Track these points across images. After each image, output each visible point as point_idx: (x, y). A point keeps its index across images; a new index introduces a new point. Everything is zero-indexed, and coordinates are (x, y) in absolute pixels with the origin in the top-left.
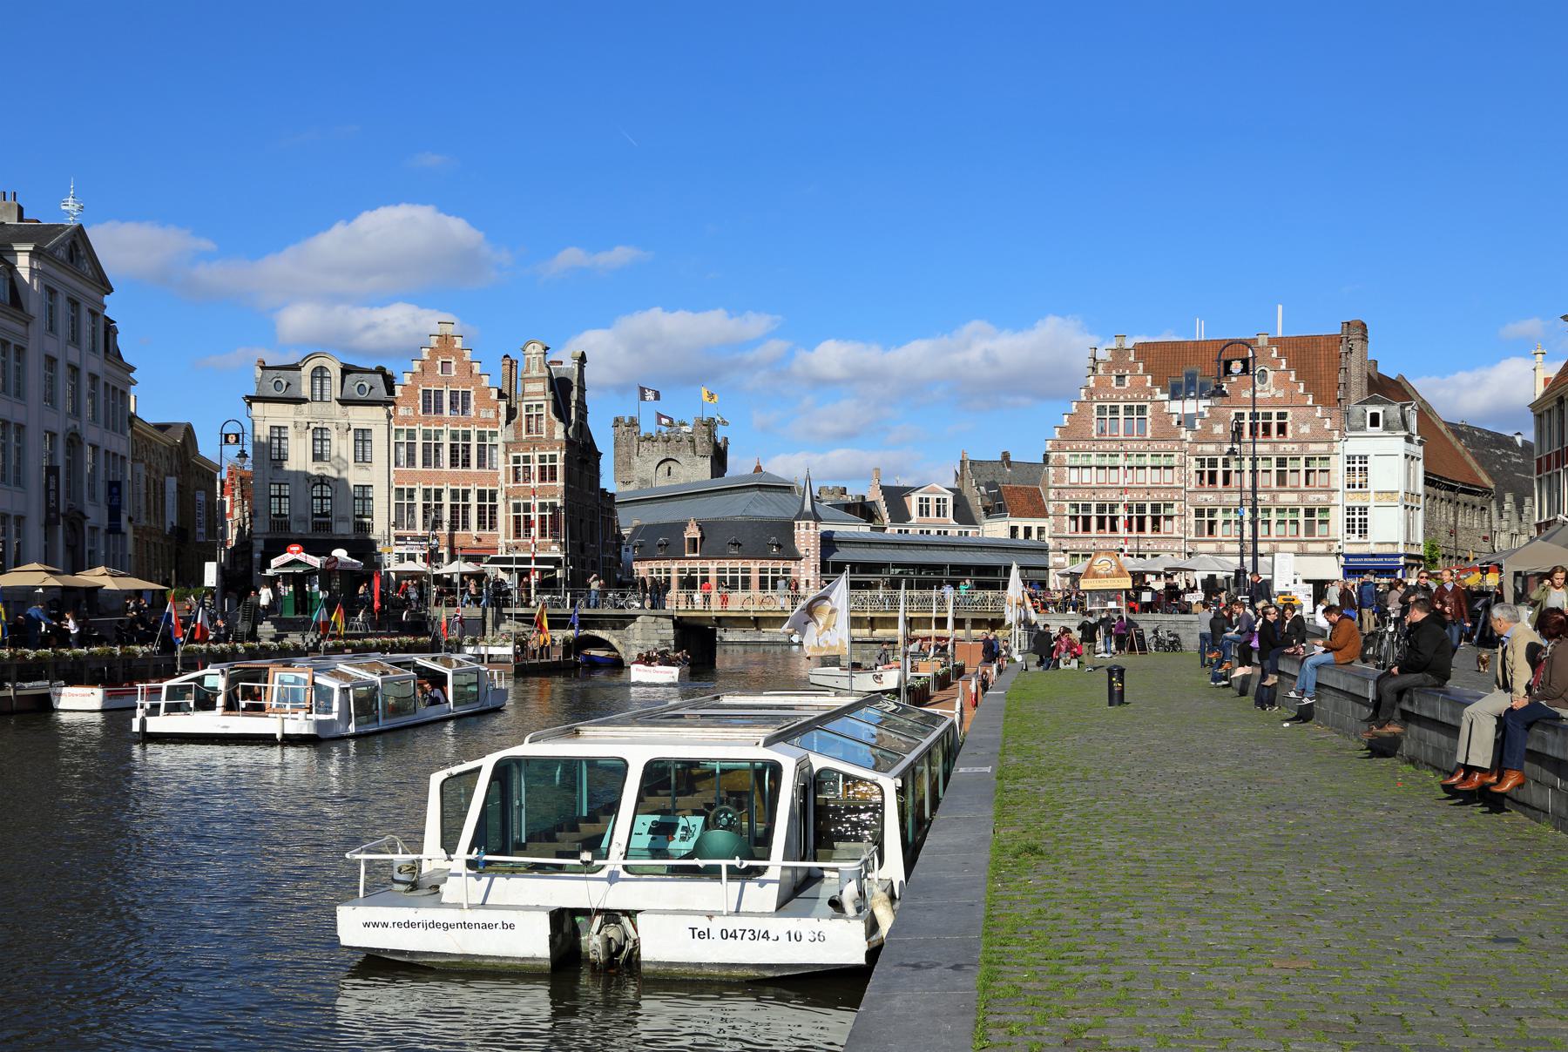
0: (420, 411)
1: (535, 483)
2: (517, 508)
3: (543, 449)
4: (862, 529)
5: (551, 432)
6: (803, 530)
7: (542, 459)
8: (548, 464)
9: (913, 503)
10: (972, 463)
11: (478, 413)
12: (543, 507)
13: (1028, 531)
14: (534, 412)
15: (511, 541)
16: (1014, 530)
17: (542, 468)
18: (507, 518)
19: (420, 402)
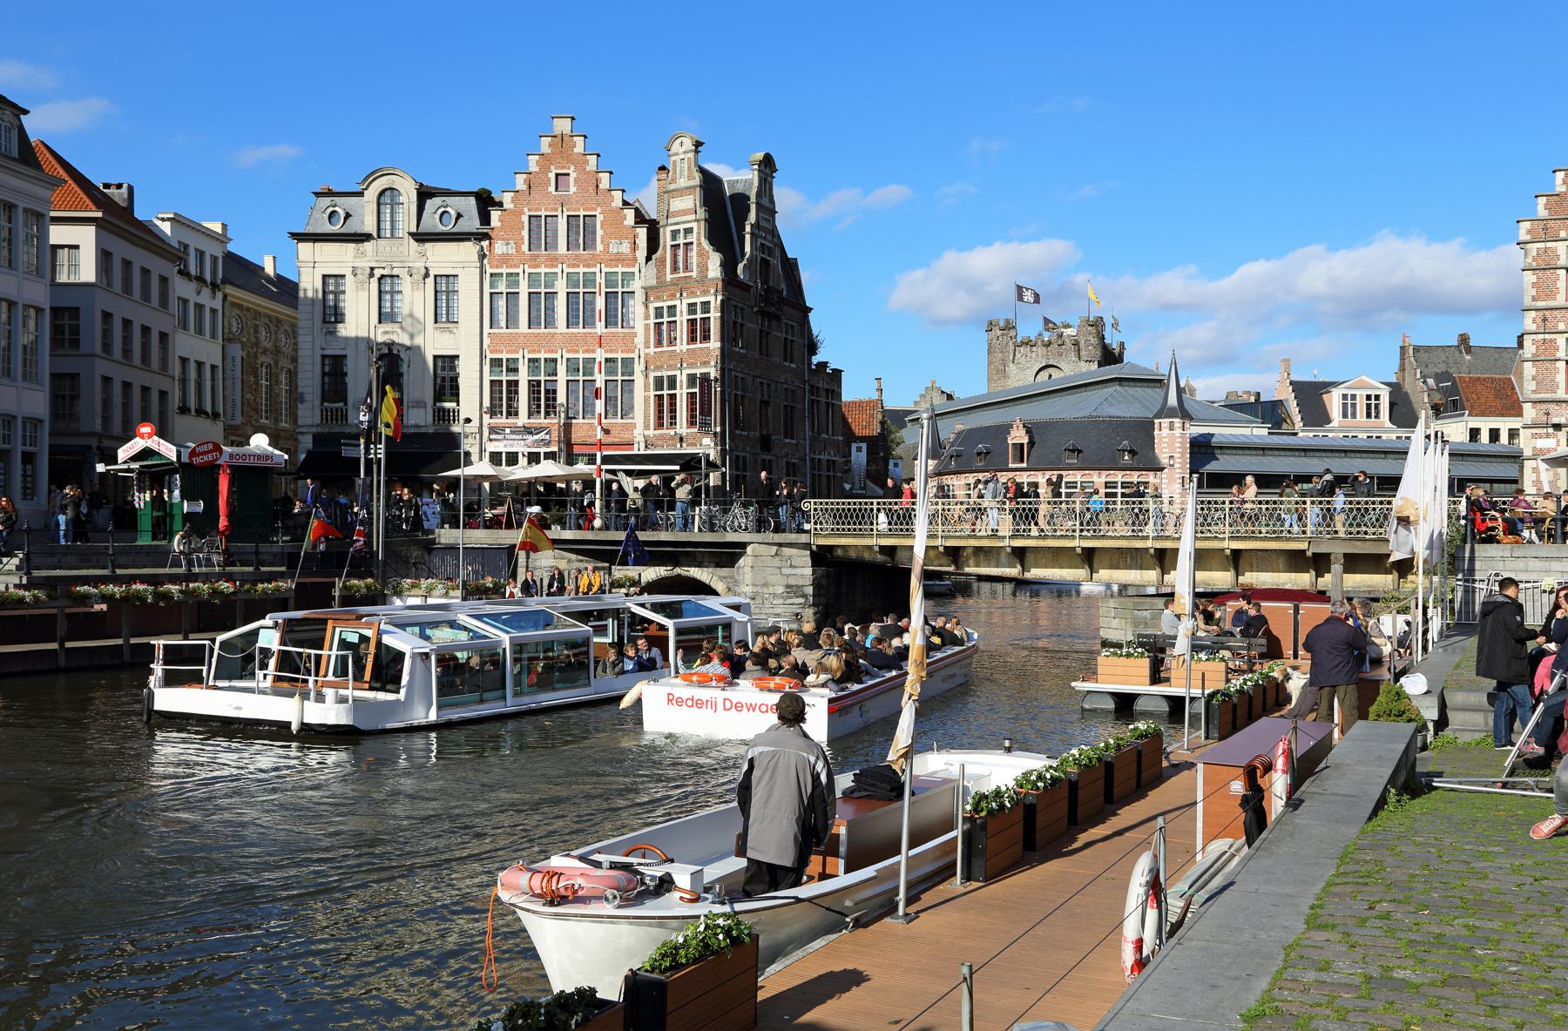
0: (525, 247)
1: (682, 346)
2: (659, 383)
3: (693, 294)
4: (1258, 432)
5: (703, 269)
6: (1166, 431)
7: (692, 308)
8: (699, 316)
9: (1334, 401)
10: (1417, 349)
11: (607, 246)
12: (692, 379)
13: (1494, 435)
14: (681, 241)
15: (651, 432)
16: (1474, 434)
17: (692, 322)
18: (646, 399)
19: (525, 233)
